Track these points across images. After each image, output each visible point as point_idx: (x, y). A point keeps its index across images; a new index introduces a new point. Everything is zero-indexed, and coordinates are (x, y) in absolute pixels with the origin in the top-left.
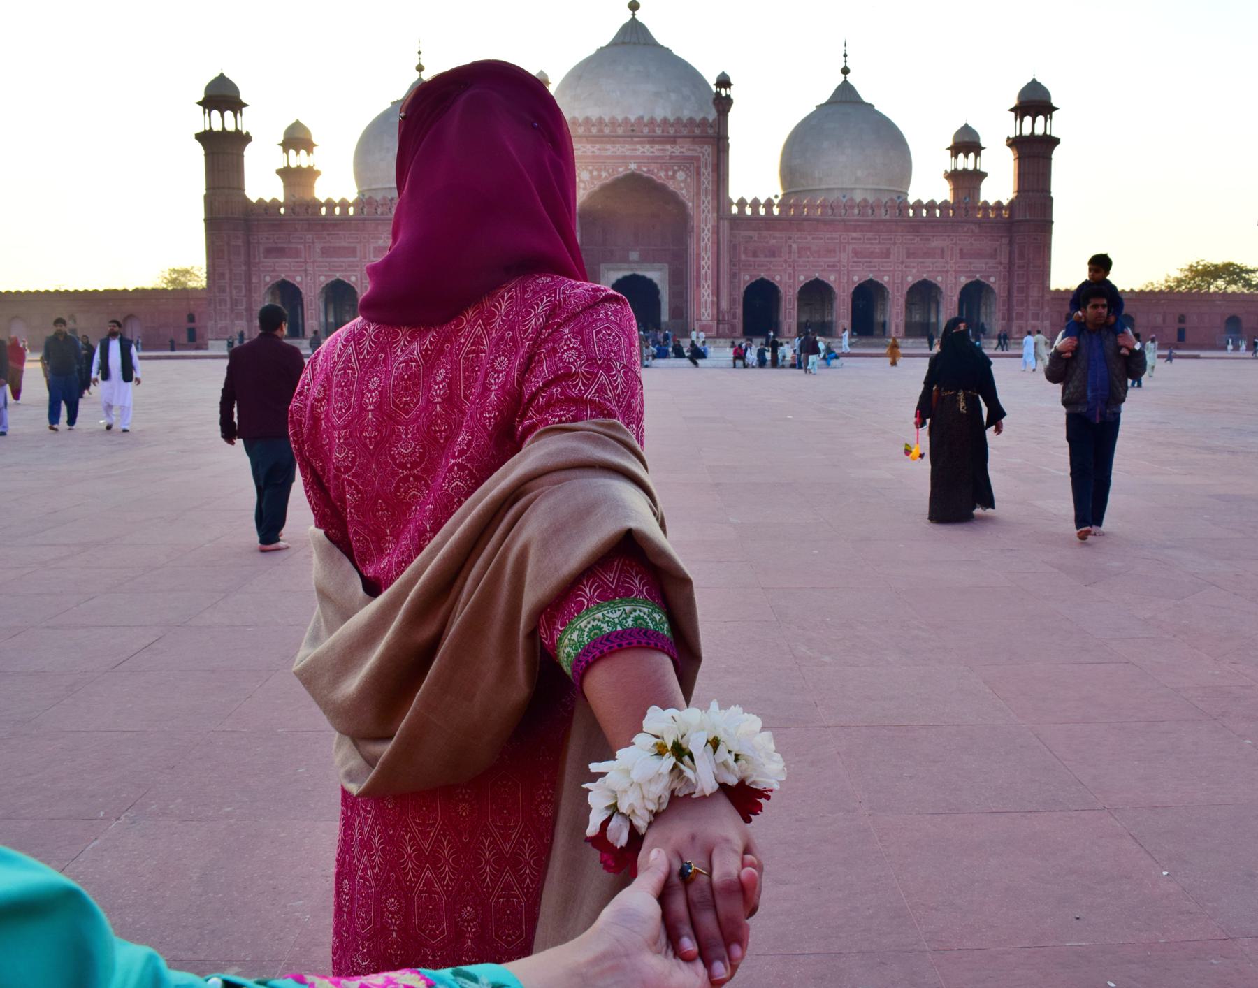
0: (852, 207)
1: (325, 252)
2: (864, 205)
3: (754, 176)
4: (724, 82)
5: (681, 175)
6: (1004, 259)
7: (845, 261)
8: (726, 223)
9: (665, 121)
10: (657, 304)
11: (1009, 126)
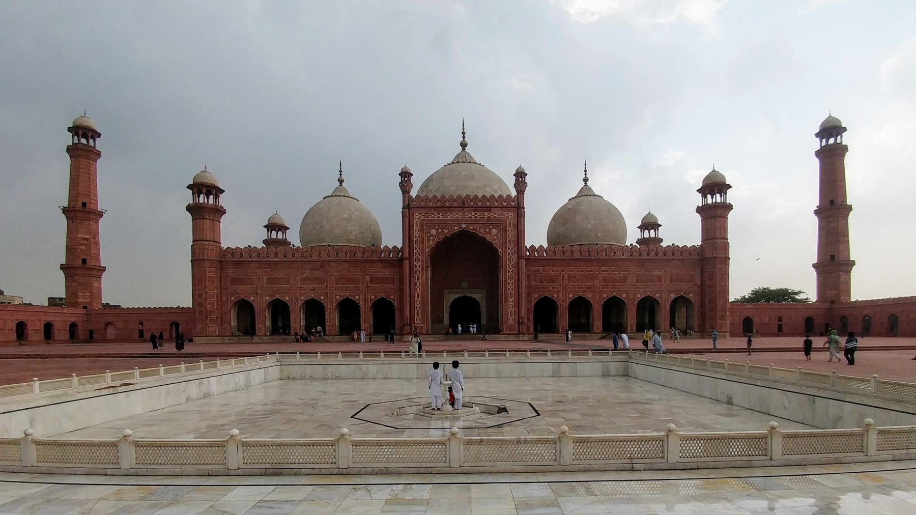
0: (602, 251)
1: (272, 280)
3: (536, 235)
4: (520, 176)
5: (494, 231)
7: (598, 285)
8: (524, 261)
10: (480, 313)
11: (698, 200)
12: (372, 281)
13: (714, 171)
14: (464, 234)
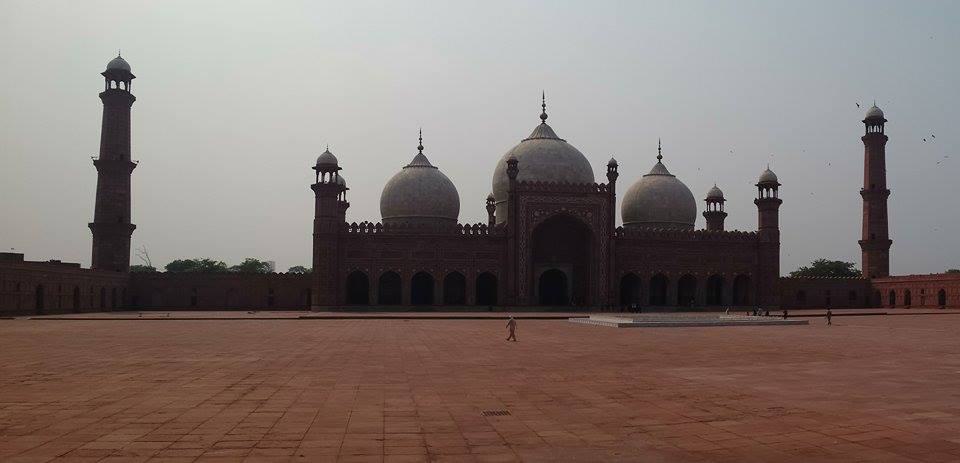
4: (613, 165)
5: (590, 214)
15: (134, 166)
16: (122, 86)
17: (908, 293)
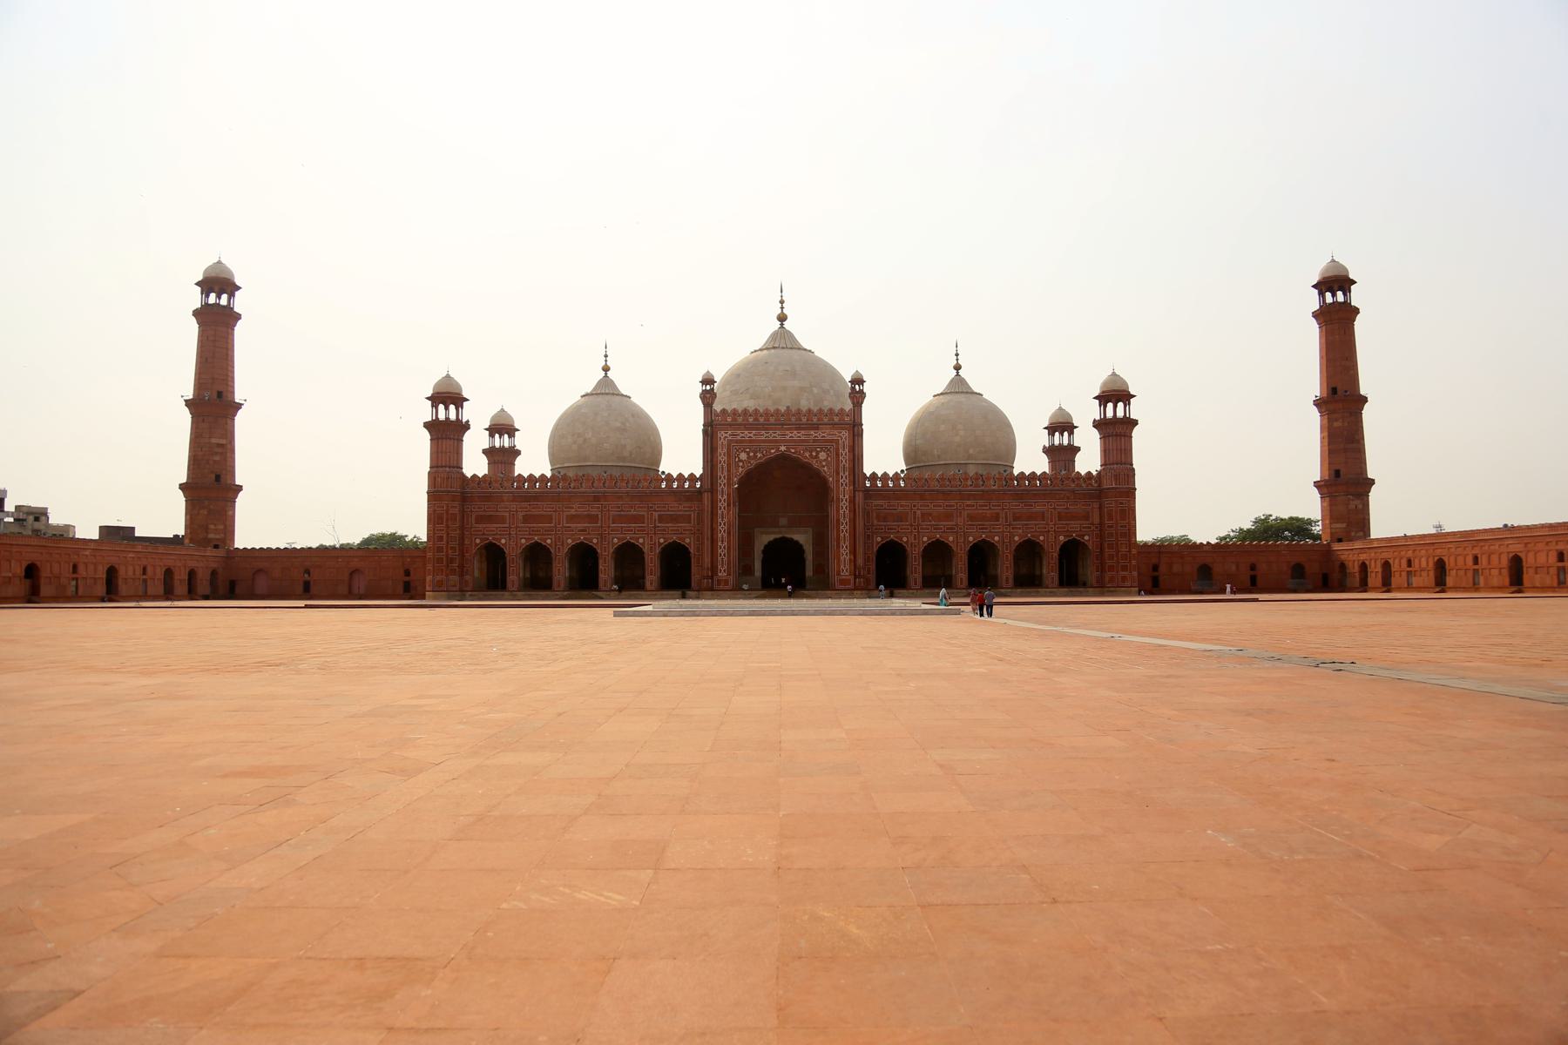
1: (527, 519)
2: (978, 477)
3: (883, 454)
5: (822, 456)
6: (1097, 520)
9: (809, 411)
10: (803, 561)
11: (1094, 412)
12: (661, 519)
13: (1114, 374)
14: (783, 459)
15: (239, 406)
16: (224, 300)
17: (1386, 565)
